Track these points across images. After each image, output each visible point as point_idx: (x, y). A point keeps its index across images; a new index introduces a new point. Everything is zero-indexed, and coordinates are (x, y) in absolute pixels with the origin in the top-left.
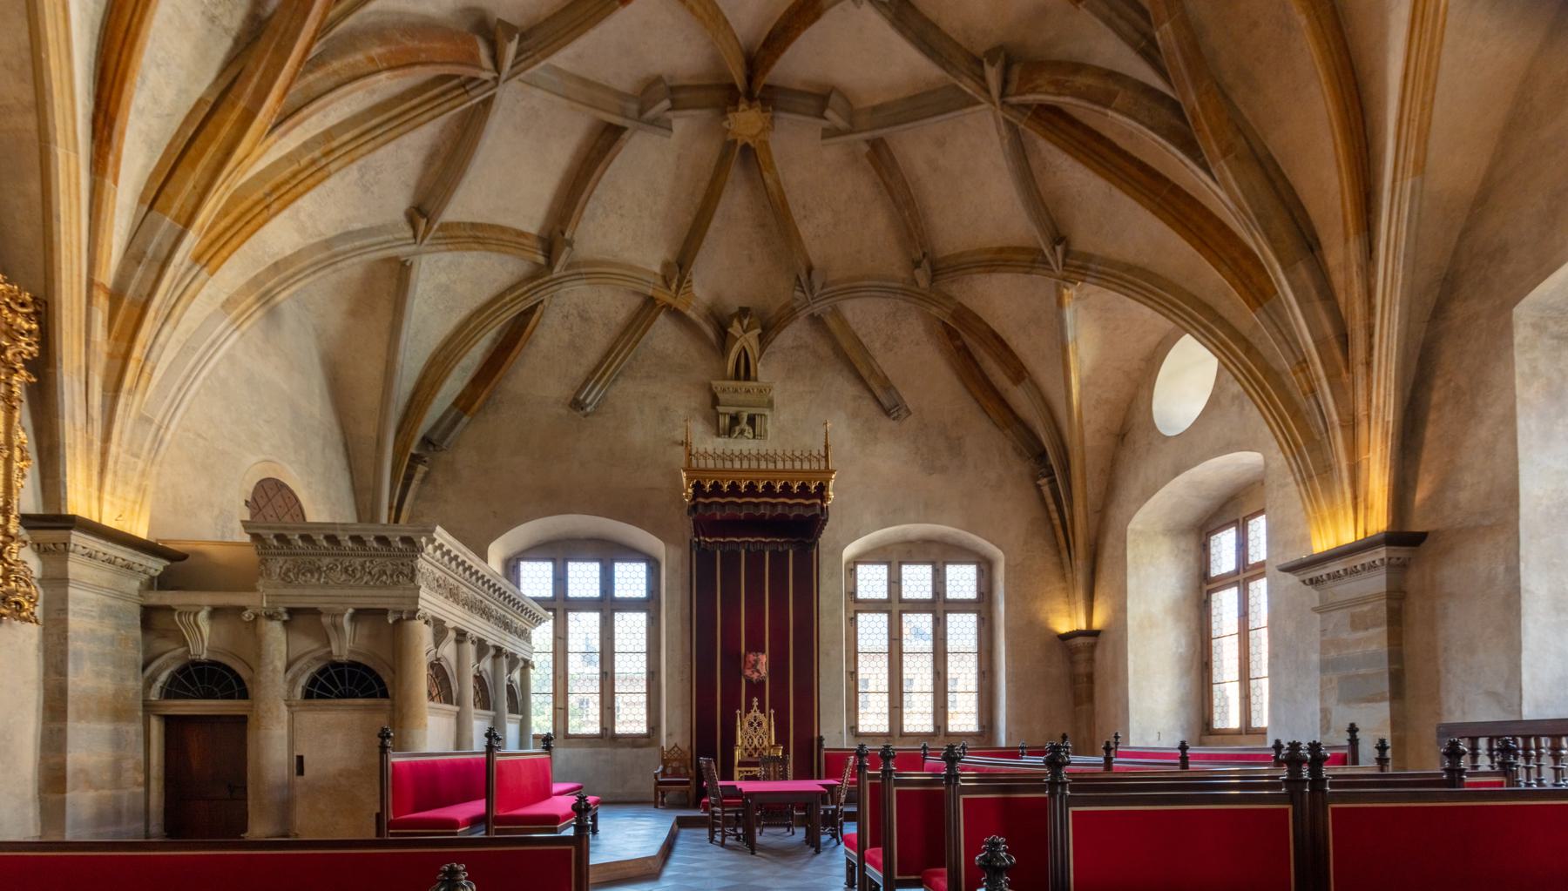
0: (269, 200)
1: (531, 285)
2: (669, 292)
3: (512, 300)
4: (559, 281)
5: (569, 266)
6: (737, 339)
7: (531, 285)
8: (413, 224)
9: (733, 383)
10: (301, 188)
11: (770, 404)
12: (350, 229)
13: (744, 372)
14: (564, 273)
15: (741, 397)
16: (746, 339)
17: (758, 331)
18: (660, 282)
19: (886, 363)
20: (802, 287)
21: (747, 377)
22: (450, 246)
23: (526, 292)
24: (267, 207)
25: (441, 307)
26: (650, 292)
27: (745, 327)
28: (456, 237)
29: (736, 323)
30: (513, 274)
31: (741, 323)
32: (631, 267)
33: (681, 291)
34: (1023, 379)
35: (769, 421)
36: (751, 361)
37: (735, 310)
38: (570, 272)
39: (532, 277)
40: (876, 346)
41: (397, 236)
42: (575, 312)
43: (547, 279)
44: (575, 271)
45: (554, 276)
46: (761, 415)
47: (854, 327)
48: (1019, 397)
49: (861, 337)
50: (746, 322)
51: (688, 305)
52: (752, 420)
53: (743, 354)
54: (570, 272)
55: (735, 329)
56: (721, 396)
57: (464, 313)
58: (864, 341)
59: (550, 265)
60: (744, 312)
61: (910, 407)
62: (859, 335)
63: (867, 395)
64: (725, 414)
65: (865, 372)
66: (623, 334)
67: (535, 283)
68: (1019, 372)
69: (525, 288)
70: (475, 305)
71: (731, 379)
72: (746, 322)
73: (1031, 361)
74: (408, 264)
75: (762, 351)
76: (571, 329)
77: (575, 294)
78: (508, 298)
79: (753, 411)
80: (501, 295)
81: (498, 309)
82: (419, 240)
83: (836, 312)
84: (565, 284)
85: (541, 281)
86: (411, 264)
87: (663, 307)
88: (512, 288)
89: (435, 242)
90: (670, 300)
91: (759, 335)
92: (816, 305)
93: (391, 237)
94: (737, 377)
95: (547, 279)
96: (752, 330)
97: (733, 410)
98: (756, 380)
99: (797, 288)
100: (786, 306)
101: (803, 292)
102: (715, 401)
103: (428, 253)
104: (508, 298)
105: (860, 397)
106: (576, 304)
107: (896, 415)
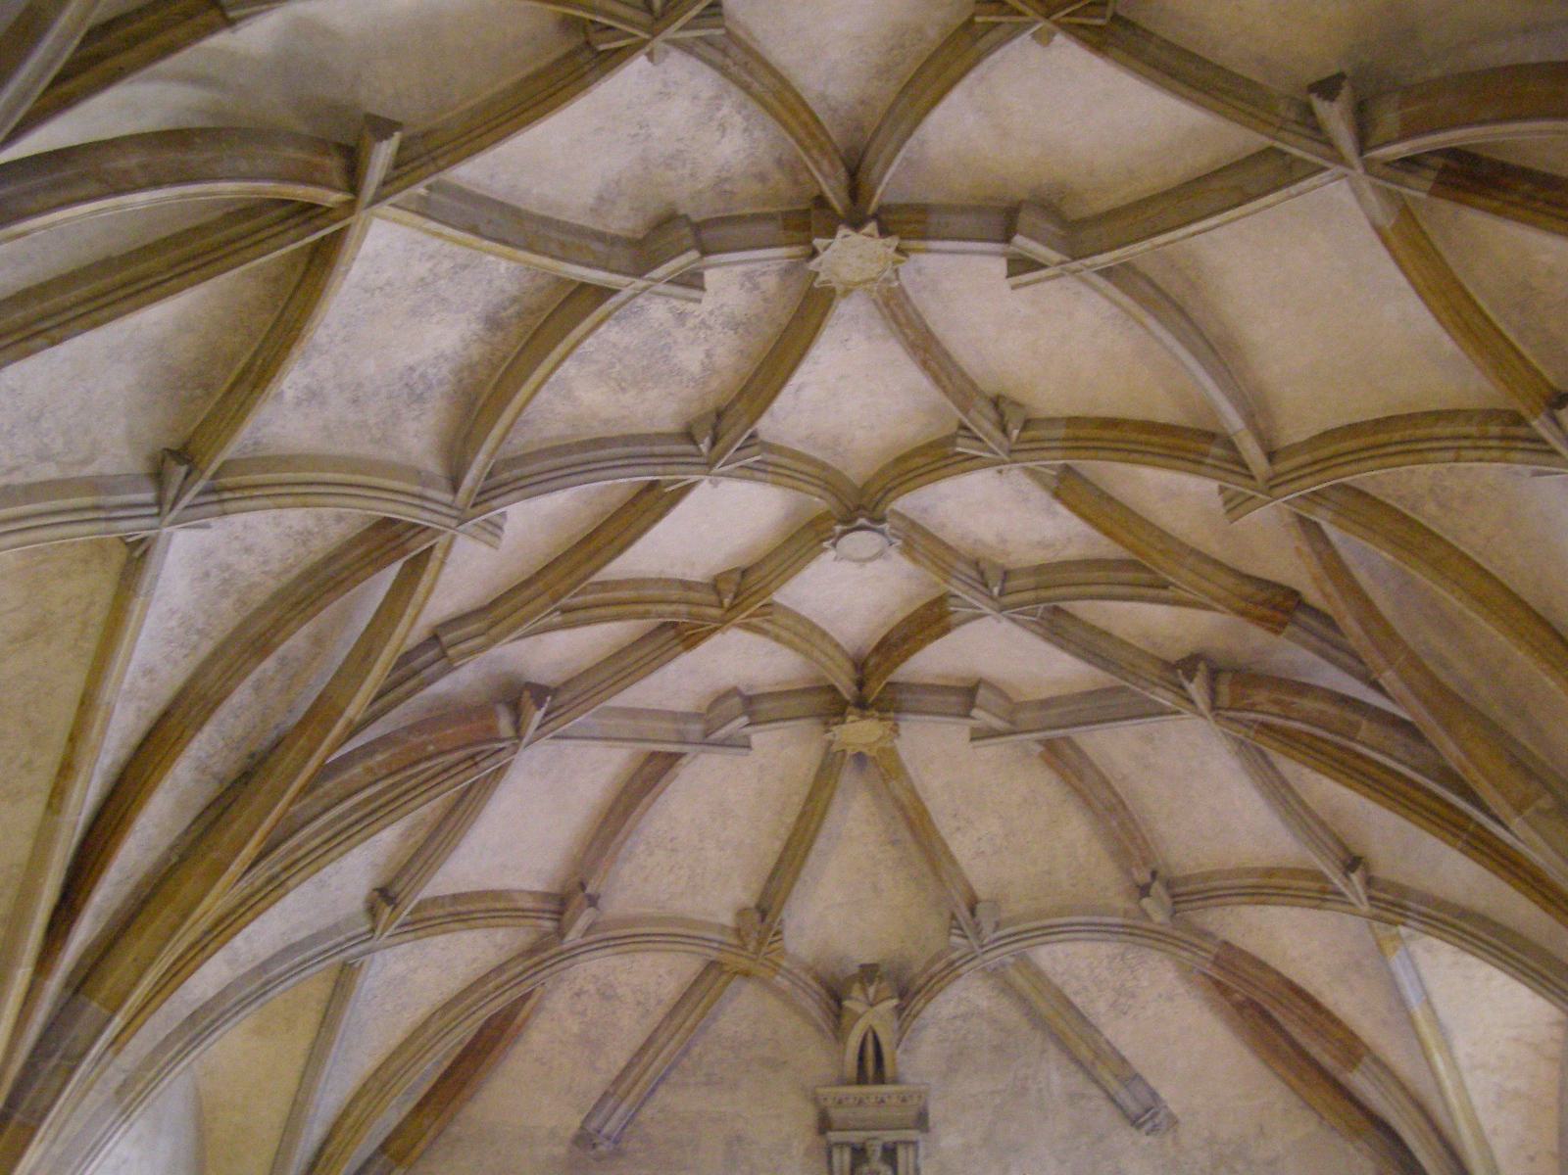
0: (205, 941)
1: (529, 963)
2: (745, 953)
3: (497, 988)
4: (573, 953)
5: (589, 930)
6: (857, 1017)
7: (529, 963)
8: (372, 910)
9: (855, 1090)
10: (249, 915)
11: (921, 1121)
12: (293, 941)
13: (872, 1066)
14: (580, 941)
15: (869, 1112)
16: (872, 1014)
17: (895, 1002)
18: (733, 940)
19: (1123, 1034)
20: (961, 929)
21: (880, 1079)
22: (420, 933)
23: (521, 974)
24: (203, 949)
25: (388, 1007)
26: (714, 955)
28: (429, 919)
29: (856, 991)
30: (502, 947)
31: (864, 990)
32: (683, 921)
33: (765, 949)
34: (1359, 1058)
35: (922, 1152)
36: (886, 1049)
37: (854, 969)
38: (590, 938)
39: (532, 951)
40: (1098, 1008)
41: (349, 934)
42: (591, 988)
43: (553, 951)
44: (599, 936)
45: (566, 946)
46: (907, 1143)
47: (1057, 981)
48: (1360, 1081)
49: (1072, 998)
51: (776, 968)
52: (890, 1154)
53: (870, 1037)
54: (590, 938)
55: (854, 1004)
56: (837, 1114)
57: (423, 1011)
58: (1077, 1001)
59: (561, 933)
60: (869, 973)
61: (1174, 1108)
62: (1068, 991)
63: (1094, 1090)
64: (841, 1145)
65: (1085, 1053)
66: (671, 1015)
67: (536, 959)
68: (1353, 1048)
69: (520, 968)
70: (439, 998)
71: (849, 1084)
73: (1366, 1027)
74: (357, 965)
75: (902, 1030)
76: (583, 1013)
77: (592, 968)
78: (491, 986)
79: (890, 1137)
80: (482, 981)
81: (475, 1003)
82: (378, 933)
83: (1024, 962)
84: (580, 958)
85: (545, 955)
86: (361, 965)
87: (736, 973)
88: (499, 969)
89: (398, 931)
90: (744, 963)
91: (896, 1007)
92: (987, 956)
93: (341, 938)
94: (861, 1079)
95: (553, 951)
96: (882, 1001)
97: (856, 1137)
98: (895, 1081)
99: (954, 931)
100: (939, 957)
101: (966, 937)
102: (824, 1125)
103: (388, 947)
104: (491, 986)
105: (1083, 1096)
106: (594, 976)
107: (1149, 1126)
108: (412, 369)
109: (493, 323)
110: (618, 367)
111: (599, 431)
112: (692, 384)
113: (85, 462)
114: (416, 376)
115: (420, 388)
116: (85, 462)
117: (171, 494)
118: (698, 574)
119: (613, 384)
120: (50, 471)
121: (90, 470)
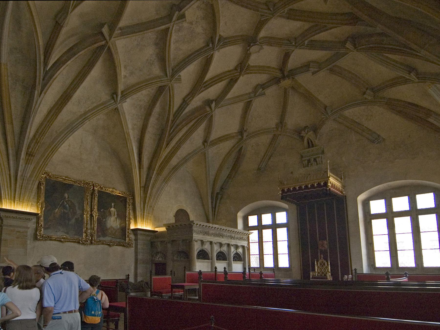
6: (305, 136)
13: (310, 144)
27: (306, 132)
29: (303, 132)
50: (306, 131)
60: (305, 127)
72: (306, 131)
108: (148, 60)
109: (156, 44)
110: (186, 39)
111: (190, 53)
112: (203, 34)
113: (100, 101)
114: (149, 61)
115: (151, 62)
116: (100, 101)
117: (115, 98)
118: (231, 68)
119: (187, 43)
120: (95, 105)
121: (102, 101)
